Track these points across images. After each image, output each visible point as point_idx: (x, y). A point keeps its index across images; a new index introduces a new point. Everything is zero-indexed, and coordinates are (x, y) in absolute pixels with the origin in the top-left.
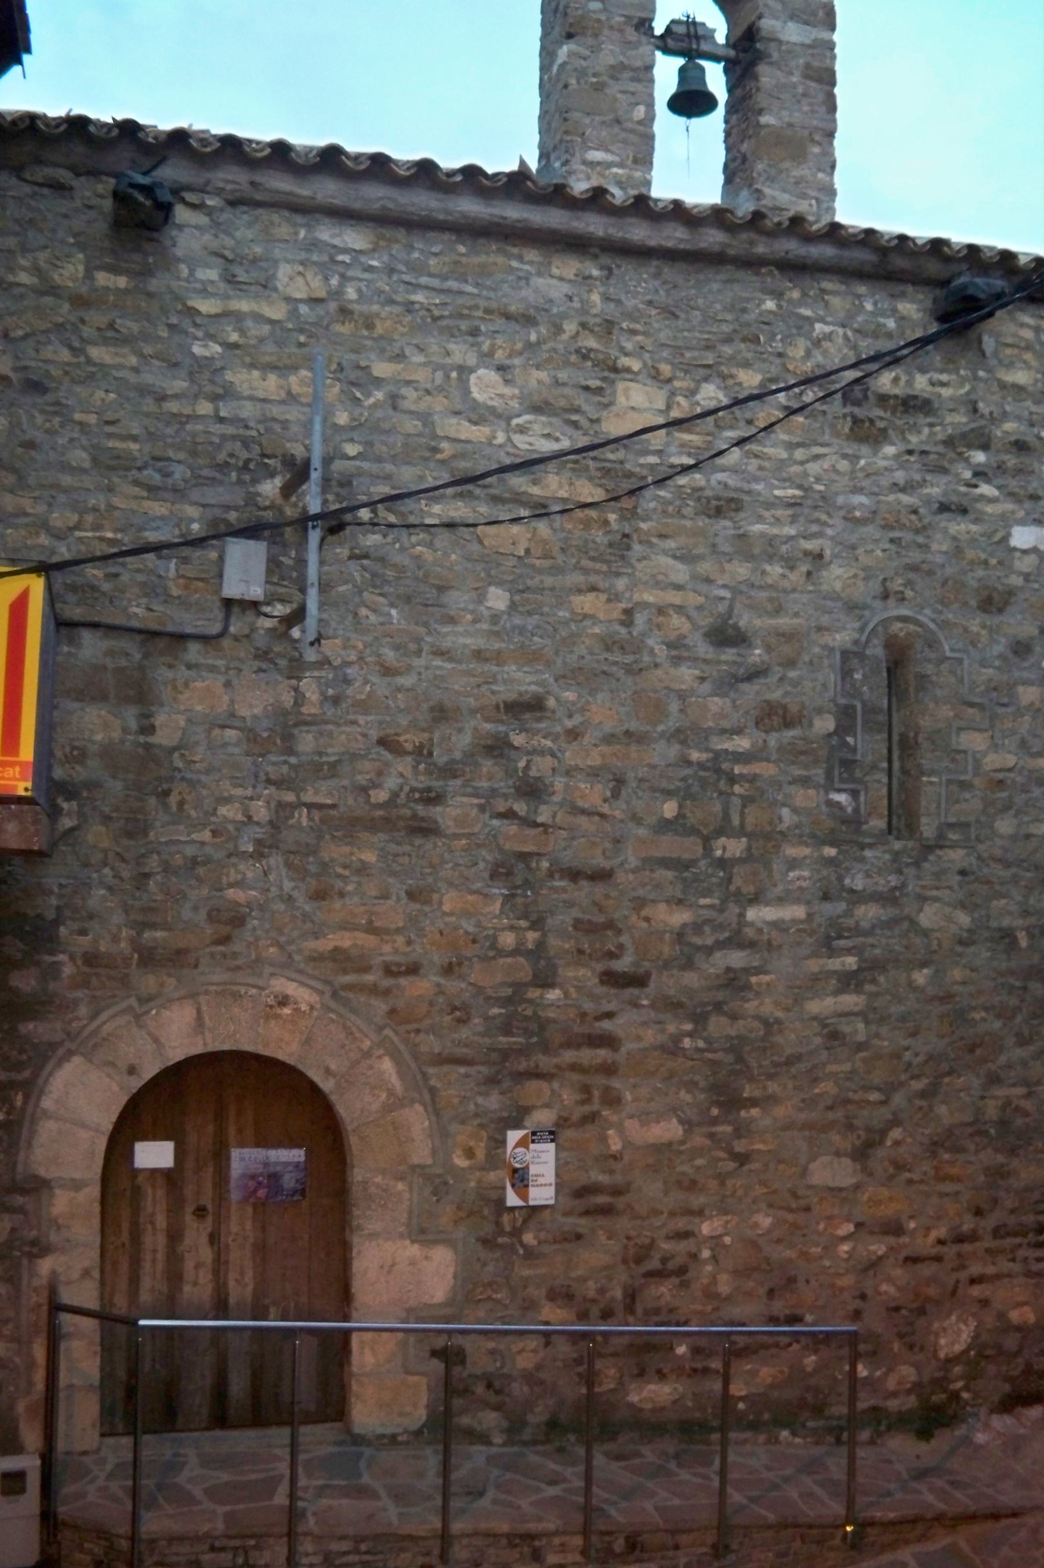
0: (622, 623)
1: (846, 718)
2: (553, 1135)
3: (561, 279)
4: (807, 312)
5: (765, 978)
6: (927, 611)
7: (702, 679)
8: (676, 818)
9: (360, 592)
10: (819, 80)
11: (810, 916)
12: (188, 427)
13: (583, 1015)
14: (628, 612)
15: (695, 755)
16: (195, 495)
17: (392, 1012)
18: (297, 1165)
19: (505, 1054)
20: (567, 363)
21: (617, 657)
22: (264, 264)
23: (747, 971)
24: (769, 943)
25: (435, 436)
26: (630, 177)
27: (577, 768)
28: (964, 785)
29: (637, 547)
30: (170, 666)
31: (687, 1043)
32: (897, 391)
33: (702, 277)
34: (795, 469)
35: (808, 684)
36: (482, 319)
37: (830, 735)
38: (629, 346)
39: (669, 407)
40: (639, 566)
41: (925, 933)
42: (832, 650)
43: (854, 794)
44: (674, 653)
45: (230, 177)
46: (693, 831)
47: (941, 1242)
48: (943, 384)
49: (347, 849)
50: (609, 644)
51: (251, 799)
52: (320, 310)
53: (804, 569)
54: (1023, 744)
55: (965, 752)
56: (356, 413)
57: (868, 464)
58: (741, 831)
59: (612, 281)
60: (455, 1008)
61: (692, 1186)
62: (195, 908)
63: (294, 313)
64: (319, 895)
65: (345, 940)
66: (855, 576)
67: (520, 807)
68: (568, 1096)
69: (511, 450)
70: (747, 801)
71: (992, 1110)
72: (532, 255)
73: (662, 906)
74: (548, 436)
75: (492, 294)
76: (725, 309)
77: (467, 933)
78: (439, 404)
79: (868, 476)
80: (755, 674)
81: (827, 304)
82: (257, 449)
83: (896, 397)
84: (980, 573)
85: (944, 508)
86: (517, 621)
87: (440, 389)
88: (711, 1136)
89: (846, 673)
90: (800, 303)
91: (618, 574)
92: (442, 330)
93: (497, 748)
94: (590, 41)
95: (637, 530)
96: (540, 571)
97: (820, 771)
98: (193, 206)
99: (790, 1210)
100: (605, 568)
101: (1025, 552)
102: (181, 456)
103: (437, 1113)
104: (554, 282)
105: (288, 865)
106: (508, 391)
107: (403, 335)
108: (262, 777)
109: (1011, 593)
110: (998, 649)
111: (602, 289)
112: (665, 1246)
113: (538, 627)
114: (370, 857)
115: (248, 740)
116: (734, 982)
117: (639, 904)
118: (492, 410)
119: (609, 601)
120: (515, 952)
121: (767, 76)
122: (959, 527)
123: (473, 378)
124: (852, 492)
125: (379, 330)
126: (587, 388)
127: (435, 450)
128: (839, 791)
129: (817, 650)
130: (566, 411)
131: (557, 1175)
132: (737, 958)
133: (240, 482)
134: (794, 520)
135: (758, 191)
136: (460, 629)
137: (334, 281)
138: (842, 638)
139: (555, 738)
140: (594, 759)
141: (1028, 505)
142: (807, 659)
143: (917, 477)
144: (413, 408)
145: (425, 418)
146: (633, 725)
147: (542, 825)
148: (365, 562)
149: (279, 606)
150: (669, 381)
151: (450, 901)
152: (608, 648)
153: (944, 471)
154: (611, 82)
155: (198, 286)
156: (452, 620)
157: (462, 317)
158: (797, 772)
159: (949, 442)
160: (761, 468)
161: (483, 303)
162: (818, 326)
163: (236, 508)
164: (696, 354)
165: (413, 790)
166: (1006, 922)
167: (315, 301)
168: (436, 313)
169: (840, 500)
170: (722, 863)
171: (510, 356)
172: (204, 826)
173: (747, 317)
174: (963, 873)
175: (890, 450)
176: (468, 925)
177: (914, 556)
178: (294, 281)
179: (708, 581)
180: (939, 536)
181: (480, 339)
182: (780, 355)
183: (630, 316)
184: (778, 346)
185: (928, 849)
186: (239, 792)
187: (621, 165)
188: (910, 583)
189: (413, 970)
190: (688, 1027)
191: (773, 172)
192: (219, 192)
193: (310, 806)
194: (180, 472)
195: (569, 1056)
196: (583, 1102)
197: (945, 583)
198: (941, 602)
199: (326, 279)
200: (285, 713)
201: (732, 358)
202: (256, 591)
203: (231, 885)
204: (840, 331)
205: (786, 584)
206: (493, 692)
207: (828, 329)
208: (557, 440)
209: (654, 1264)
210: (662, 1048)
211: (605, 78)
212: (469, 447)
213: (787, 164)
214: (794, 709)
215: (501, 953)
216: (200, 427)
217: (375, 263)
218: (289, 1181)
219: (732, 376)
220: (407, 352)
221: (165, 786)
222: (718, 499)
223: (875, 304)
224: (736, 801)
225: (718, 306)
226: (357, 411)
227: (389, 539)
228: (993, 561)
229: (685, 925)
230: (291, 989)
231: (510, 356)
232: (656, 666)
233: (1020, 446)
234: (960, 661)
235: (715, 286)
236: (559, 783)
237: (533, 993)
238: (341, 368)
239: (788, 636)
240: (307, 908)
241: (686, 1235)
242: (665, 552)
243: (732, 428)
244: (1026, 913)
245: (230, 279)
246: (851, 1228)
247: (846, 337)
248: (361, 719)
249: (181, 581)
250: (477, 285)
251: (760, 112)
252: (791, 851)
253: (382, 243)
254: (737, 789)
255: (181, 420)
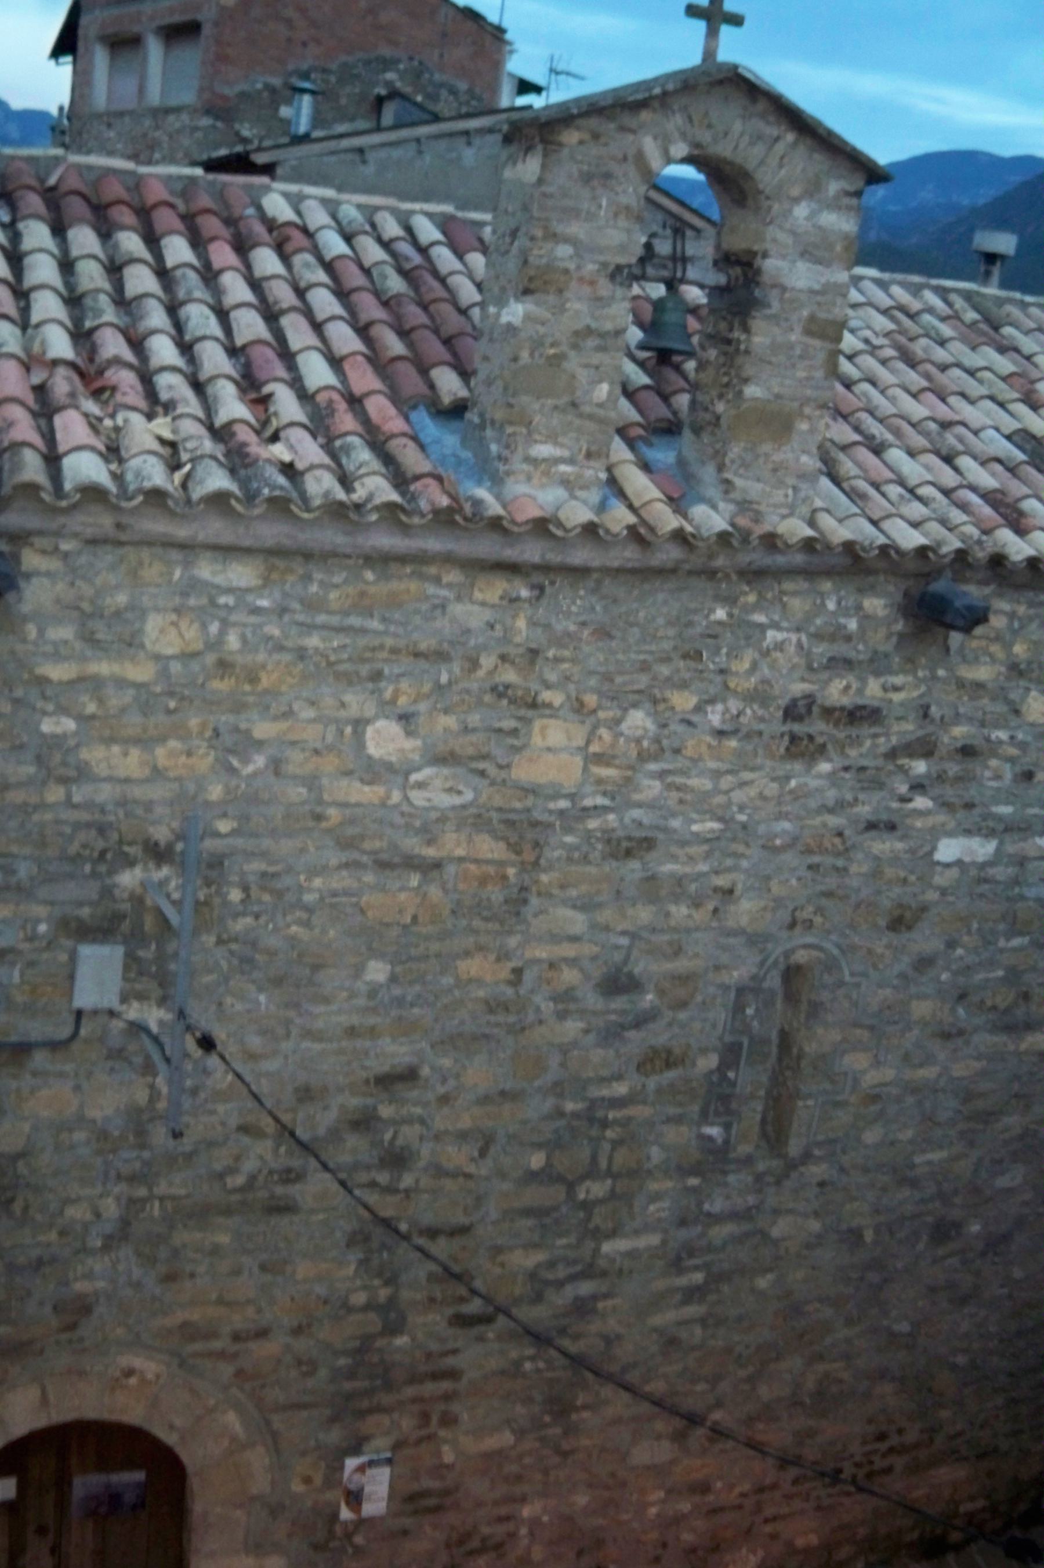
0: (511, 983)
1: (731, 1055)
2: (389, 1461)
3: (483, 604)
4: (760, 618)
5: (610, 1303)
6: (834, 937)
7: (587, 1031)
8: (542, 1170)
9: (227, 979)
10: (822, 336)
11: (664, 1242)
12: (36, 817)
13: (429, 1355)
14: (518, 972)
15: (570, 1106)
16: (43, 892)
17: (239, 1373)
18: (138, 1485)
19: (349, 1397)
20: (480, 703)
21: (501, 1018)
22: (129, 615)
23: (595, 1298)
24: (621, 1270)
25: (320, 802)
26: (579, 476)
27: (446, 1132)
28: (837, 1104)
29: (534, 901)
30: (15, 1077)
31: (528, 1366)
32: (846, 701)
33: (647, 586)
34: (720, 799)
35: (697, 1025)
36: (385, 661)
37: (711, 1072)
38: (552, 677)
39: (588, 742)
40: (535, 922)
41: (776, 1243)
42: (726, 988)
43: (727, 1127)
44: (560, 1007)
45: (91, 520)
46: (560, 1179)
47: (743, 1495)
48: (896, 689)
49: (198, 1235)
50: (493, 1006)
51: (101, 1196)
52: (195, 666)
53: (710, 907)
54: (906, 1058)
55: (846, 1074)
56: (234, 782)
57: (799, 786)
58: (610, 1173)
59: (544, 601)
60: (300, 1363)
61: (519, 1478)
62: (41, 1303)
63: (164, 673)
64: (170, 1278)
65: (194, 1315)
66: (765, 909)
67: (383, 1178)
68: (407, 1423)
69: (405, 808)
70: (616, 1144)
71: (810, 1384)
72: (453, 576)
73: (519, 1252)
74: (450, 790)
75: (401, 630)
76: (670, 623)
77: (319, 1297)
78: (329, 764)
79: (796, 799)
80: (642, 1020)
81: (784, 606)
82: (115, 836)
83: (842, 709)
84: (897, 890)
85: (871, 826)
86: (397, 991)
87: (330, 748)
88: (542, 1439)
89: (738, 1008)
90: (756, 607)
91: (510, 933)
92: (338, 676)
93: (363, 1122)
94: (551, 299)
95: (537, 882)
96: (428, 938)
97: (696, 1108)
98: (44, 552)
99: (607, 1488)
100: (497, 926)
101: (948, 865)
102: (27, 850)
103: (277, 1451)
104: (476, 608)
105: (139, 1254)
106: (409, 744)
107: (291, 686)
108: (113, 1173)
109: (924, 909)
110: (897, 969)
111: (529, 612)
112: (486, 1530)
113: (419, 996)
114: (224, 1239)
115: (98, 1140)
116: (583, 1308)
117: (497, 1250)
118: (389, 767)
119: (498, 960)
120: (367, 1307)
121: (762, 335)
122: (883, 846)
123: (370, 731)
124: (777, 819)
125: (265, 682)
126: (500, 730)
127: (319, 818)
128: (712, 1124)
129: (712, 990)
130: (472, 758)
131: (391, 1487)
132: (586, 1288)
133: (94, 874)
134: (708, 855)
135: (727, 482)
136: (334, 1007)
137: (214, 628)
138: (737, 975)
139: (426, 1105)
140: (465, 1122)
141: (961, 814)
142: (699, 998)
143: (849, 797)
144: (298, 771)
145: (311, 782)
146: (508, 1086)
147: (407, 1192)
148: (234, 946)
149: (136, 1004)
150: (594, 711)
151: (303, 1269)
152: (491, 1011)
153: (881, 786)
154: (572, 354)
155: (49, 648)
156: (326, 1000)
157: (363, 660)
158: (672, 1111)
159: (892, 754)
160: (681, 801)
161: (389, 642)
162: (771, 634)
163: (91, 903)
164: (627, 678)
165: (271, 1172)
166: (855, 1223)
167: (187, 656)
168: (333, 658)
169: (762, 829)
170: (587, 1206)
171: (415, 701)
172: (51, 1226)
173: (691, 632)
174: (822, 1184)
175: (825, 767)
176: (320, 1290)
177: (831, 882)
178: (164, 634)
179: (607, 928)
180: (860, 856)
181: (383, 684)
182: (722, 671)
183: (560, 640)
184: (722, 659)
185: (792, 1166)
186: (87, 1192)
187: (571, 461)
188: (820, 910)
189: (262, 1334)
190: (530, 1351)
191: (749, 457)
192: (76, 535)
193: (162, 1199)
194: (24, 870)
195: (410, 1391)
196: (420, 1427)
197: (858, 906)
198: (852, 926)
199: (204, 626)
200: (139, 1111)
201: (668, 679)
202: (111, 1000)
203: (76, 1279)
204: (794, 637)
205: (691, 924)
206: (364, 1068)
207: (780, 636)
208: (459, 793)
209: (475, 1543)
210: (503, 1372)
211: (564, 348)
212: (359, 811)
213: (766, 447)
214: (677, 1051)
215: (350, 1310)
216: (48, 816)
217: (264, 603)
218: (129, 1498)
219: (665, 700)
220: (296, 707)
221: (9, 1194)
222: (629, 838)
223: (839, 603)
224: (607, 1147)
225: (661, 621)
226: (234, 782)
227: (262, 920)
228: (912, 878)
229: (539, 1265)
230: (138, 1362)
231: (415, 701)
232: (541, 1022)
233: (967, 751)
234: (858, 985)
235: (661, 597)
236: (426, 1151)
237: (380, 1343)
238: (217, 733)
239: (684, 979)
240: (158, 1291)
241: (508, 1518)
242: (564, 902)
243: (656, 757)
244: (877, 1212)
245: (90, 639)
246: (662, 1494)
247: (800, 645)
248: (221, 1108)
249: (26, 987)
250: (384, 620)
251: (746, 381)
252: (653, 1186)
253: (275, 576)
254: (609, 1134)
255: (25, 809)
